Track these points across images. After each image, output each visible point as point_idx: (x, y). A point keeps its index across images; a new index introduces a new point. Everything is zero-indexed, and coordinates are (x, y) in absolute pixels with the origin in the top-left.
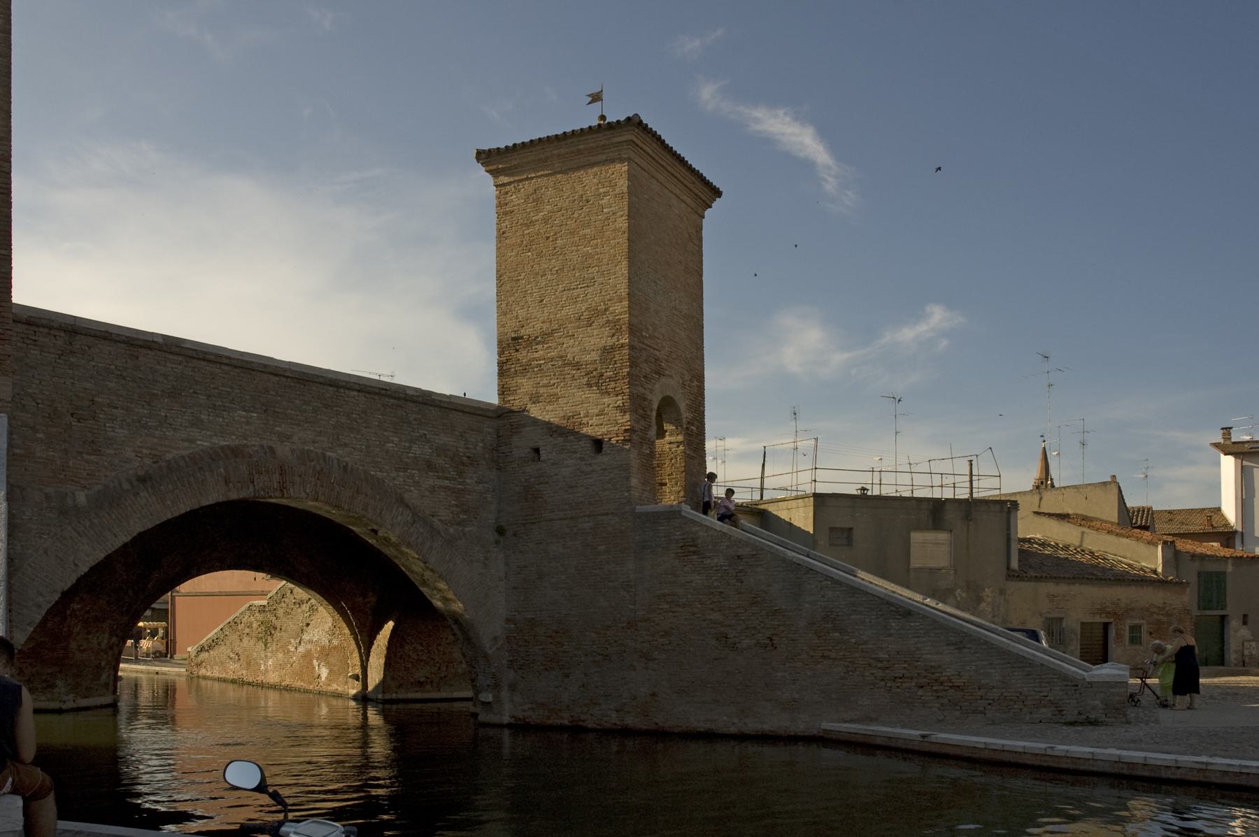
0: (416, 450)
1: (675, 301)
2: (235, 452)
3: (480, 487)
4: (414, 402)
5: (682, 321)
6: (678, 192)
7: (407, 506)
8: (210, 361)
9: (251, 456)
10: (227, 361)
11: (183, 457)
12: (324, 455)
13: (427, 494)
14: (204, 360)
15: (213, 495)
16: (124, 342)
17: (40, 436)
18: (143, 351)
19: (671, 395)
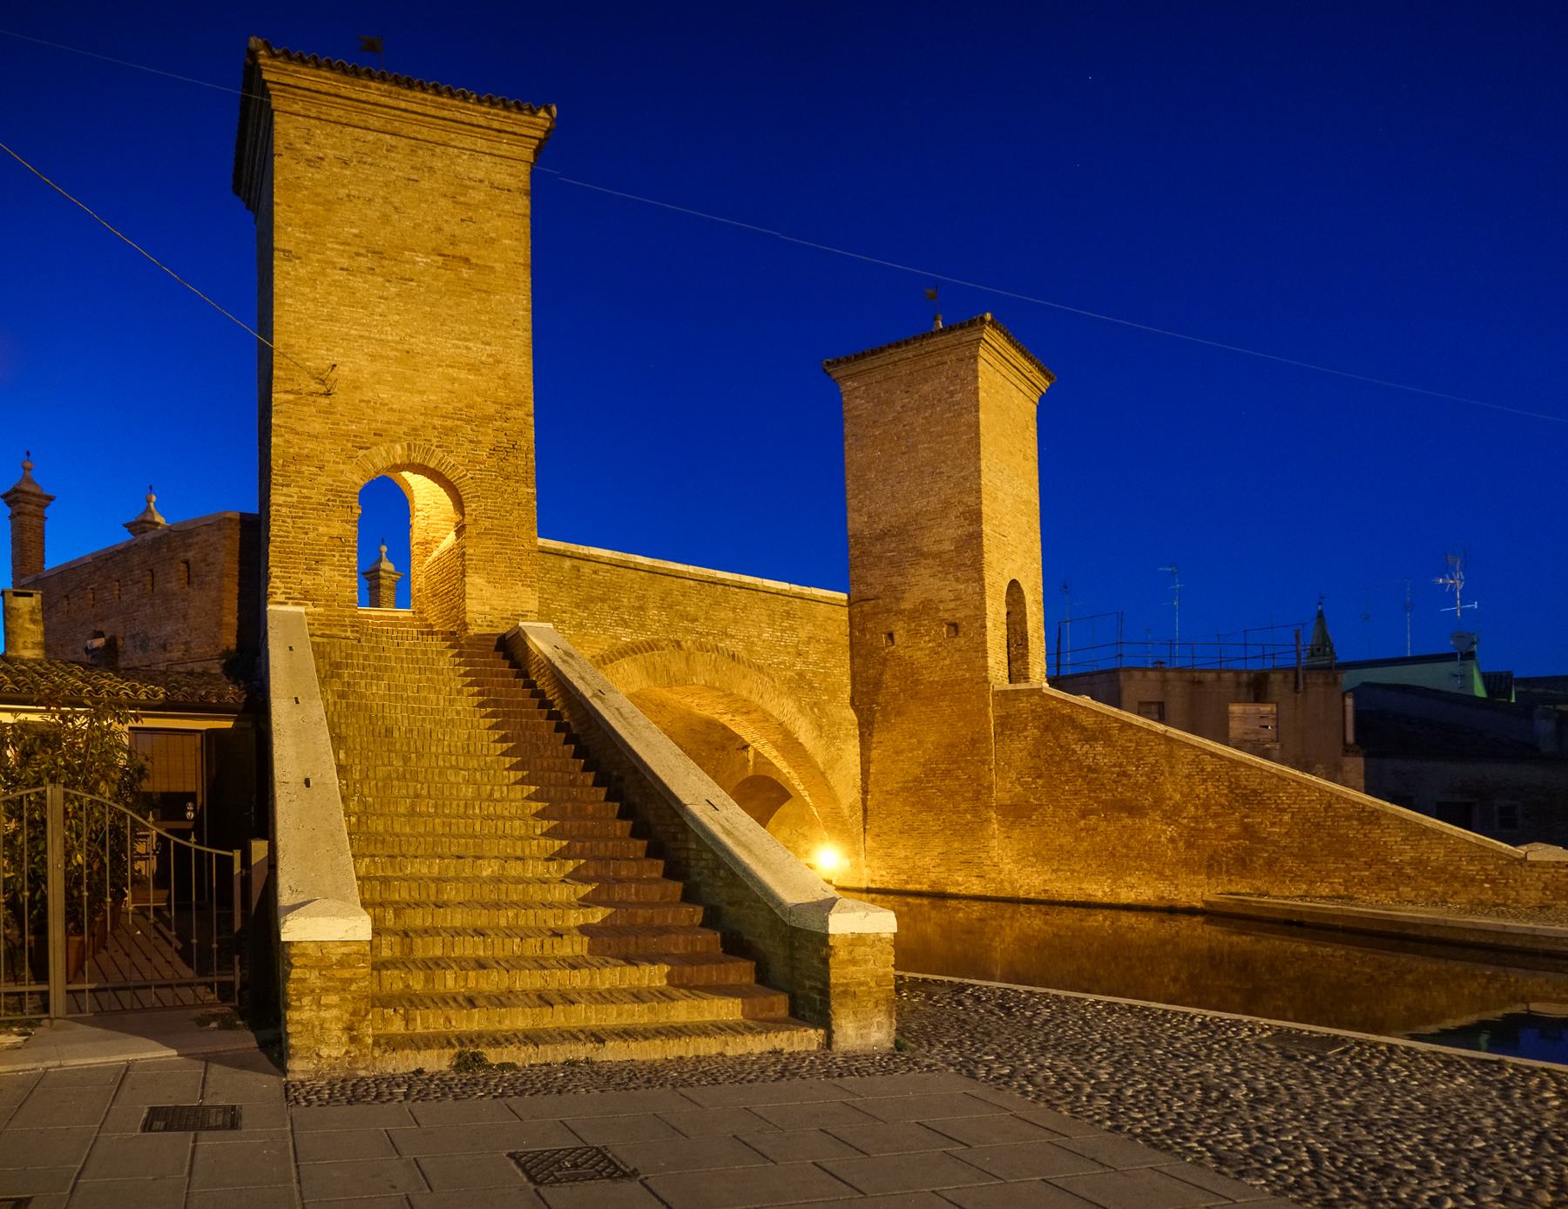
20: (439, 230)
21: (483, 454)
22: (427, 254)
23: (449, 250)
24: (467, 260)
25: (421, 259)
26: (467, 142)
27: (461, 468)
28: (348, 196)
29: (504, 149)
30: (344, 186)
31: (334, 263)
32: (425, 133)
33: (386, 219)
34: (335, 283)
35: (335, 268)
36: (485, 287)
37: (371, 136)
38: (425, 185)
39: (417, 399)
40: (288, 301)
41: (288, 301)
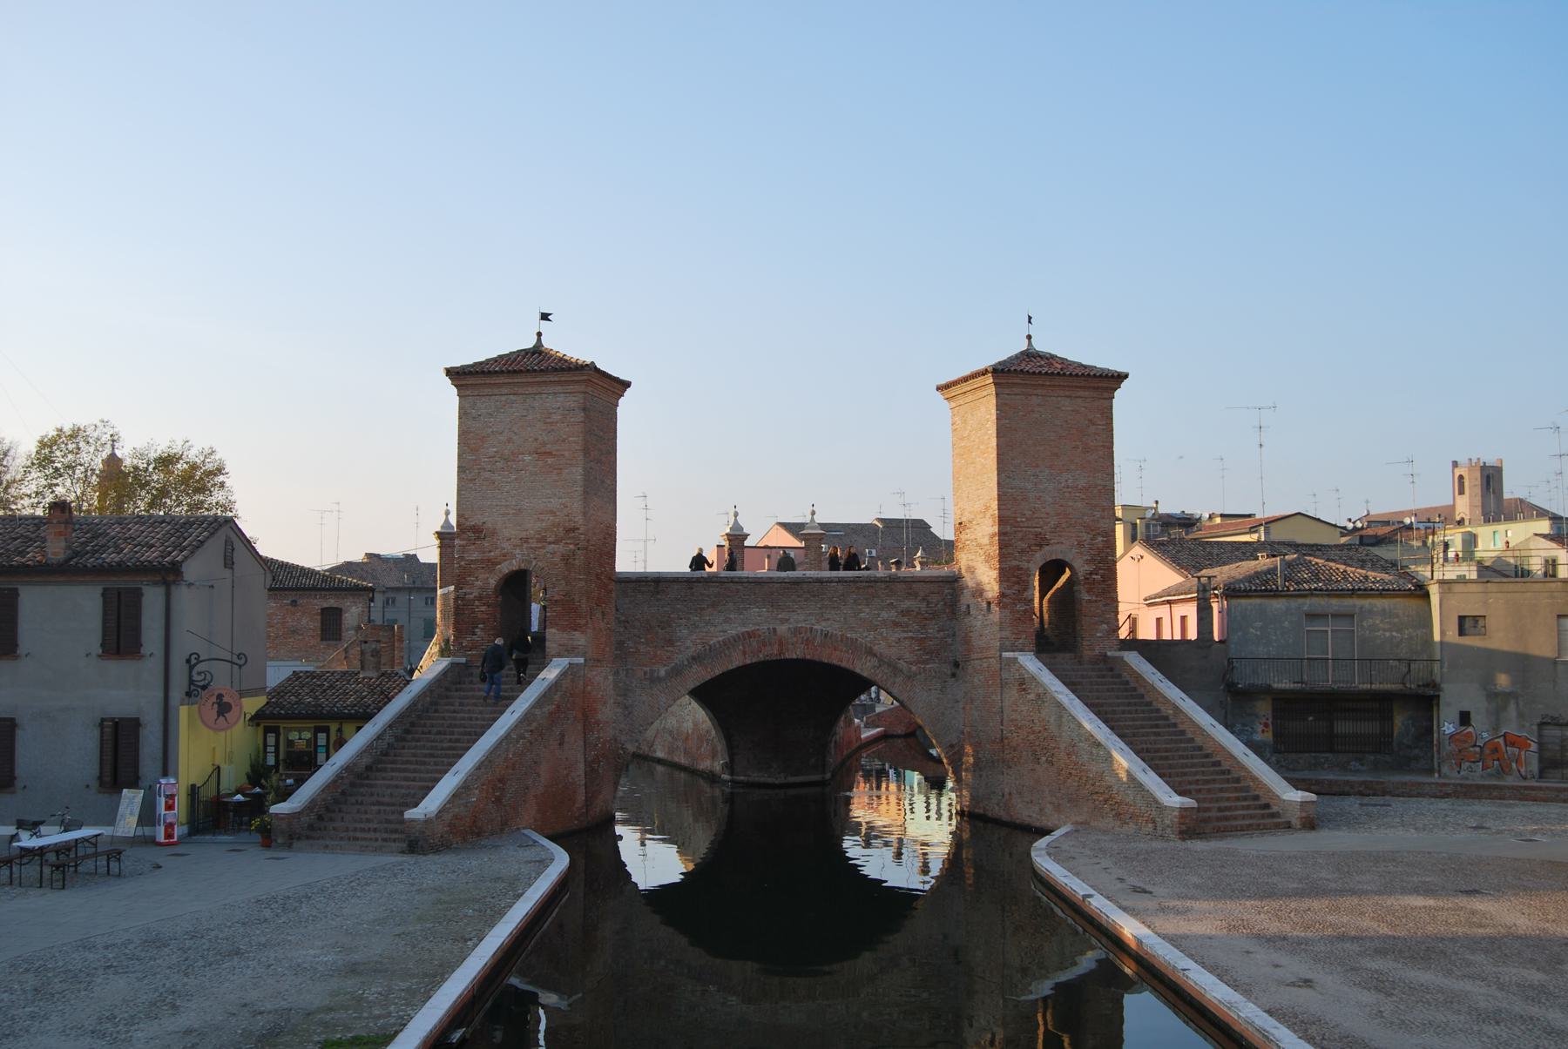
0: (884, 615)
1: (1066, 481)
2: (750, 635)
3: (942, 633)
4: (882, 582)
5: (1078, 494)
6: (1067, 393)
7: (875, 655)
8: (737, 583)
9: (760, 636)
10: (746, 580)
11: (719, 642)
12: (811, 629)
13: (893, 644)
14: (731, 582)
15: (737, 660)
16: (685, 581)
17: (642, 640)
18: (696, 584)
19: (1060, 557)
20: (536, 440)
21: (557, 559)
22: (530, 454)
23: (543, 450)
24: (550, 454)
25: (527, 458)
26: (551, 389)
27: (546, 568)
28: (492, 432)
29: (570, 388)
30: (490, 427)
31: (484, 469)
32: (530, 390)
33: (509, 440)
34: (486, 480)
35: (485, 471)
36: (561, 466)
37: (503, 398)
38: (530, 417)
39: (525, 533)
40: (463, 492)
41: (463, 492)
